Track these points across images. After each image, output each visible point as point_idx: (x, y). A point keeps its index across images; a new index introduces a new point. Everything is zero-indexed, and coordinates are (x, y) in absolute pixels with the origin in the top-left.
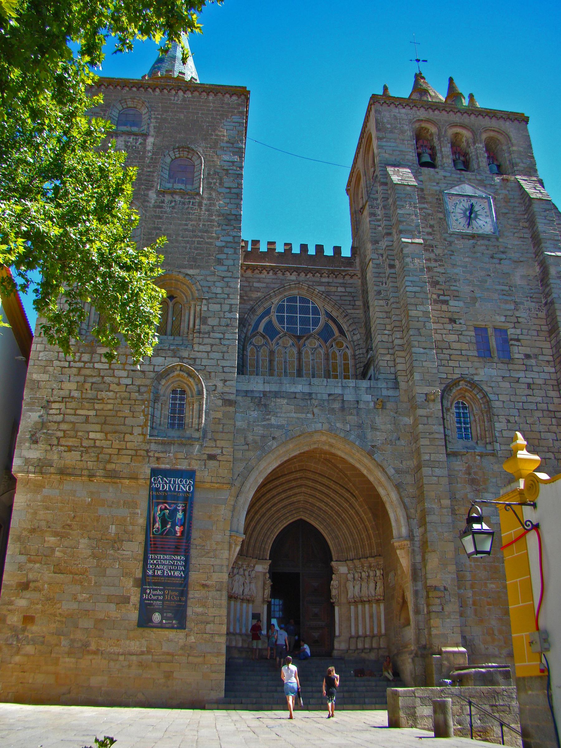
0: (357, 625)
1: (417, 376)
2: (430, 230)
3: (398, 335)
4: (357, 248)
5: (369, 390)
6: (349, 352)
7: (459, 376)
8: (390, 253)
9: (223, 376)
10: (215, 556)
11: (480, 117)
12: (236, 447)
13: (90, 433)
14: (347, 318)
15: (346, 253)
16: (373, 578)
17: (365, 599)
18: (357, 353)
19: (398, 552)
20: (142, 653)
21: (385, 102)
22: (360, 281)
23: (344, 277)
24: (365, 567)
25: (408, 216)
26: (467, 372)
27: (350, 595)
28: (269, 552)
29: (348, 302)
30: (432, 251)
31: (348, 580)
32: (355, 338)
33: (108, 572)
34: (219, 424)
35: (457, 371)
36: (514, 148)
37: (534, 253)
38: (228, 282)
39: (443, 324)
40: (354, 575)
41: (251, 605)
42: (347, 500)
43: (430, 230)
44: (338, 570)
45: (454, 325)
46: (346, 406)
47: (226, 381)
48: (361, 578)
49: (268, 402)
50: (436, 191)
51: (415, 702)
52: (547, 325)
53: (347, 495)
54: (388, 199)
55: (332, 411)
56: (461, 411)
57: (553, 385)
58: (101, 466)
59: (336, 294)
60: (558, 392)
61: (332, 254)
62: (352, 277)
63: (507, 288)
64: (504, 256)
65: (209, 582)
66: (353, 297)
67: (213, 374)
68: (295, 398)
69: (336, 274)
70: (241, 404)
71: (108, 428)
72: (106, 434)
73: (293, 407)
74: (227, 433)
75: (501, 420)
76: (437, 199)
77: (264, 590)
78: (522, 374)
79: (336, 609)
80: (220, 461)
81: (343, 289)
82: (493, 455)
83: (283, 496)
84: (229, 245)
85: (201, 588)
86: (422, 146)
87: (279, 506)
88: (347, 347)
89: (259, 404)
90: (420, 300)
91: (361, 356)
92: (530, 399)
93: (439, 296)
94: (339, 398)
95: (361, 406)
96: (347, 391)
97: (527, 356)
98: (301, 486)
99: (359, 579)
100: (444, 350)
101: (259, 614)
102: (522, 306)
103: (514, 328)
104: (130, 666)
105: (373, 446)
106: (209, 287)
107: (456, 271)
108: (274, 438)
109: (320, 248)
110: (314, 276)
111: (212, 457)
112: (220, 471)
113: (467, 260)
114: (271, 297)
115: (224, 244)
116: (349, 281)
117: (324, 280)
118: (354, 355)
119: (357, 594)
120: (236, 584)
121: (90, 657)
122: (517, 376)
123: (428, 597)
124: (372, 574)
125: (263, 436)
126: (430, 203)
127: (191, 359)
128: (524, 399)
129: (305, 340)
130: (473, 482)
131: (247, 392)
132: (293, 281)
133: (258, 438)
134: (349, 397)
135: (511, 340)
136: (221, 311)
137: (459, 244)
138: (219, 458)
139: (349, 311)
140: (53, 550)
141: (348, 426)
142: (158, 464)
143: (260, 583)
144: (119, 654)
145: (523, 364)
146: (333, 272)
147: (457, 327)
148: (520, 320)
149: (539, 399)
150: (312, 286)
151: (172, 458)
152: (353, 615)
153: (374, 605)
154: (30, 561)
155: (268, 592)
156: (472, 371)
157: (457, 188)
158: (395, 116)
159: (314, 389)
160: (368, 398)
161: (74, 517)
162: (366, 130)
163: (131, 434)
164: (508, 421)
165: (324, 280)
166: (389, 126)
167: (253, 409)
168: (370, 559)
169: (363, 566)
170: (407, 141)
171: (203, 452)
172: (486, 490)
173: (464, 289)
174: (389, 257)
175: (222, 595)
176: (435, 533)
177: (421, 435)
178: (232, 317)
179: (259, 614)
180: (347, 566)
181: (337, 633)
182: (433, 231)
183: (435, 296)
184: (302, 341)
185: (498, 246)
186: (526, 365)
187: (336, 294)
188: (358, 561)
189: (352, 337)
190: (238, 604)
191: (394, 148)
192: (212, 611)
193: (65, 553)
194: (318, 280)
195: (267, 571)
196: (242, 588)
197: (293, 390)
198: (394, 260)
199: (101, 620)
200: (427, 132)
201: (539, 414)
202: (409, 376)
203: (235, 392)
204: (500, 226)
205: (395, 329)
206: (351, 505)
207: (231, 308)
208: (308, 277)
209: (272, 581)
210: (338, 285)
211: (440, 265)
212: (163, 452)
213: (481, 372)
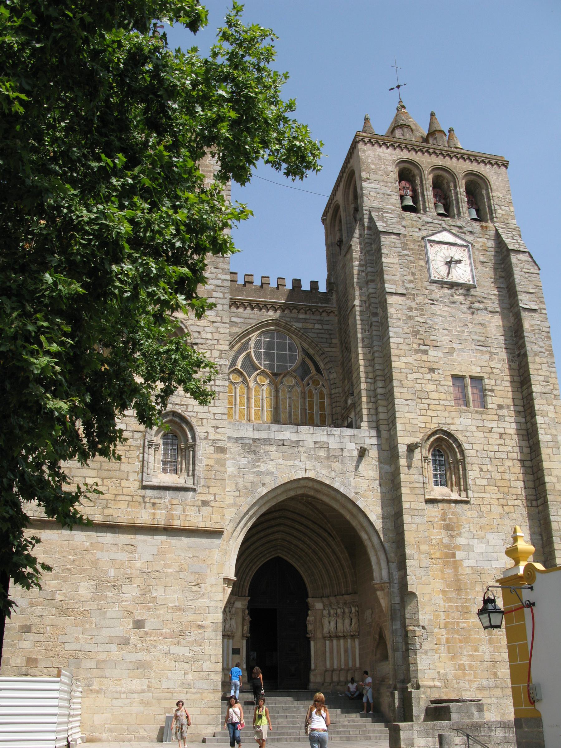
0: (332, 659)
1: (399, 427)
2: (412, 278)
3: (380, 384)
4: (334, 283)
5: (352, 438)
6: (325, 391)
7: (437, 425)
8: (373, 300)
9: (214, 423)
10: (210, 598)
11: (461, 160)
13: (87, 479)
14: (324, 356)
15: (323, 288)
17: (340, 635)
18: (333, 391)
19: (379, 593)
20: (143, 691)
21: (370, 140)
22: (336, 318)
23: (321, 314)
25: (392, 266)
26: (444, 422)
27: (326, 630)
29: (324, 340)
30: (414, 299)
31: (323, 616)
32: (332, 376)
33: (109, 614)
35: (435, 420)
36: (494, 194)
37: (510, 304)
38: (217, 328)
39: (422, 373)
41: (231, 641)
42: (324, 539)
43: (412, 278)
44: (314, 606)
45: (433, 375)
46: (331, 455)
47: (218, 428)
49: (258, 449)
50: (418, 237)
51: (413, 735)
52: (520, 376)
53: (325, 535)
54: (372, 244)
55: (318, 458)
56: (437, 458)
57: (523, 435)
58: (99, 510)
59: (313, 331)
60: (527, 442)
61: (309, 289)
62: (328, 314)
63: (483, 339)
64: (481, 306)
65: (204, 624)
66: (330, 334)
67: (204, 421)
68: (283, 445)
69: (313, 310)
70: (232, 451)
71: (104, 474)
72: (103, 479)
73: (281, 454)
75: (474, 468)
76: (419, 246)
77: (243, 625)
78: (494, 424)
79: (312, 643)
80: (213, 507)
81: (320, 327)
82: (467, 502)
83: (262, 534)
84: (219, 289)
85: (197, 629)
86: (404, 188)
87: (258, 544)
88: (323, 386)
89: (249, 451)
90: (403, 351)
91: (337, 395)
92: (502, 448)
93: (420, 345)
94: (325, 446)
95: (346, 453)
96: (332, 439)
97: (500, 407)
98: (279, 525)
100: (423, 400)
101: (239, 649)
102: (496, 357)
103: (489, 378)
104: (131, 703)
105: (356, 493)
106: (199, 332)
107: (436, 320)
108: (264, 485)
109: (297, 283)
110: (291, 312)
111: (205, 503)
112: (213, 516)
113: (446, 309)
114: (249, 334)
115: (212, 287)
116: (327, 318)
117: (302, 316)
118: (331, 394)
121: (94, 695)
122: (490, 426)
124: (347, 610)
125: (253, 483)
126: (412, 249)
127: (182, 405)
128: (496, 448)
129: (283, 377)
130: (448, 527)
131: (237, 439)
132: (270, 316)
133: (248, 485)
134: (334, 444)
135: (486, 390)
136: (211, 357)
137: (439, 293)
138: (212, 504)
139: (326, 349)
140: (54, 594)
141: (333, 474)
142: (154, 509)
143: (240, 620)
144: (121, 693)
145: (496, 414)
146: (310, 308)
147: (435, 376)
148: (494, 370)
149: (510, 449)
150: (290, 322)
151: (168, 503)
152: (328, 649)
153: (349, 640)
154: (31, 604)
155: (247, 628)
156: (449, 421)
157: (438, 235)
158: (379, 156)
159: (301, 437)
160: (352, 446)
161: (74, 561)
162: (349, 166)
163: (127, 480)
164: (481, 470)
165: (302, 316)
166: (373, 167)
167: (243, 456)
168: (346, 597)
169: (338, 603)
170: (392, 183)
171: (196, 498)
172: (459, 535)
173: (443, 339)
174: (373, 305)
175: (217, 635)
176: (414, 577)
177: (403, 484)
178: (222, 363)
179: (239, 649)
180: (323, 602)
181: (313, 667)
182: (415, 279)
183: (415, 346)
184: (279, 379)
185: (475, 296)
186: (499, 416)
187: (313, 331)
188: (334, 598)
189: (328, 376)
191: (379, 191)
192: (208, 651)
193: (66, 597)
194: (295, 316)
197: (281, 436)
198: (376, 308)
199: (104, 661)
200: (410, 173)
201: (509, 463)
202: (391, 425)
203: (226, 439)
204: (478, 275)
205: (378, 378)
206: (328, 544)
207: (221, 354)
208: (286, 312)
209: (251, 617)
210: (315, 321)
211: (420, 314)
212: (159, 498)
213: (457, 421)
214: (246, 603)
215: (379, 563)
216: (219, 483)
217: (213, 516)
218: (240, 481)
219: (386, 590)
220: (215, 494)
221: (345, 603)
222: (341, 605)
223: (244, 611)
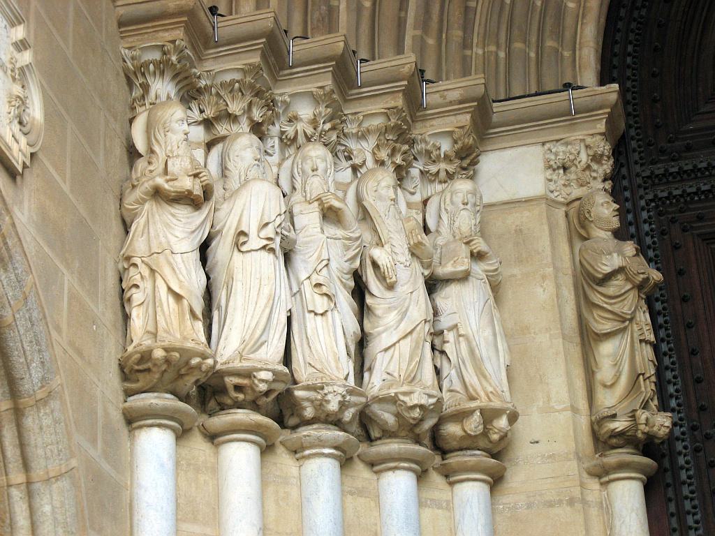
77: (588, 339)
223: (579, 226)
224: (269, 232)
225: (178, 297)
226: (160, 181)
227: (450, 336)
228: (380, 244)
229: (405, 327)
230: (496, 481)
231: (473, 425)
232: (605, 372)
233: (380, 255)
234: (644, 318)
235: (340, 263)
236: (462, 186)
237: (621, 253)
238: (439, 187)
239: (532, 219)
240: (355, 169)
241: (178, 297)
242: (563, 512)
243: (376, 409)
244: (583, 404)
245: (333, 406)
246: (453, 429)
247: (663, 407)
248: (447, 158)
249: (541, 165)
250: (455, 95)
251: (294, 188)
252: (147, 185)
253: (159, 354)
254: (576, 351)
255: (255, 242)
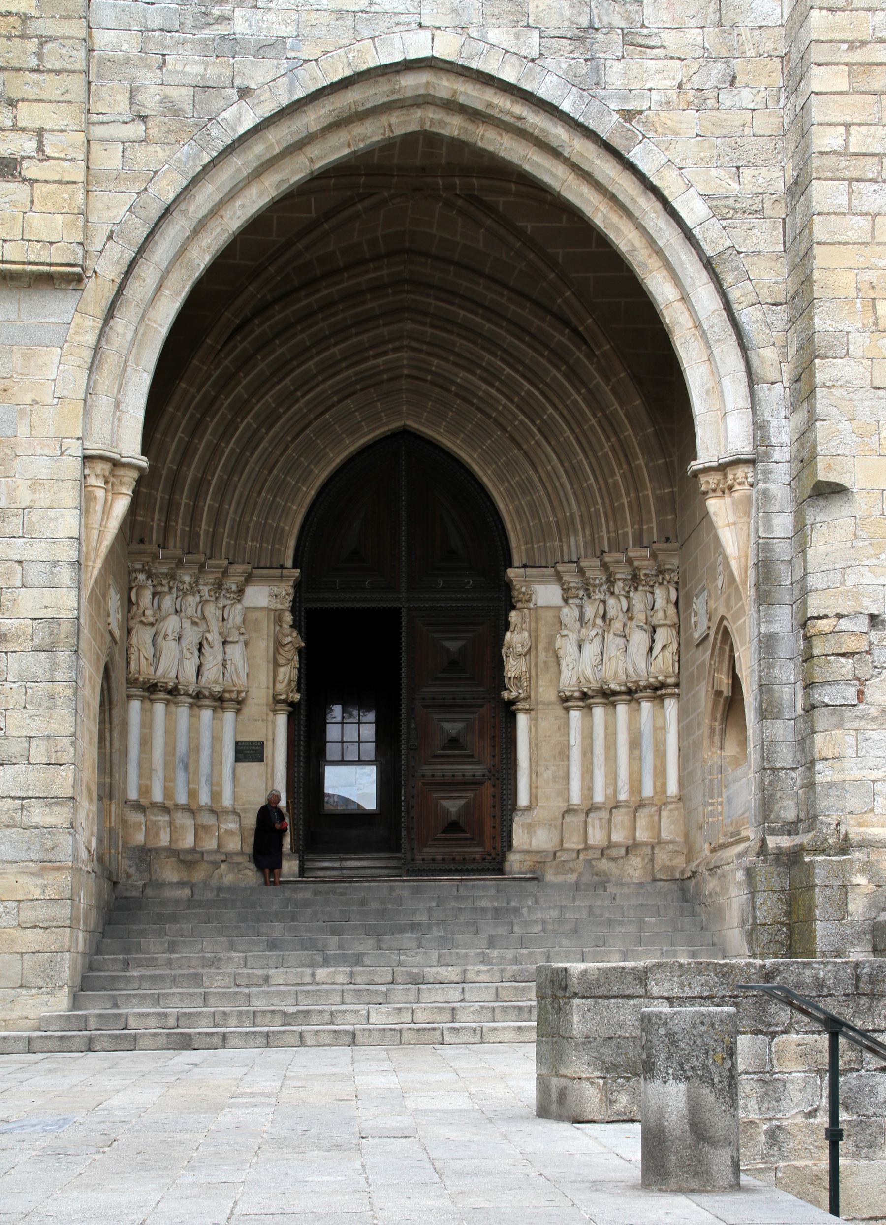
12: (99, 131)
16: (642, 617)
24: (620, 584)
28: (292, 543)
34: (23, 37)
40: (581, 607)
41: (229, 717)
48: (604, 617)
74: (58, 72)
77: (276, 665)
80: (32, 182)
99: (599, 622)
108: (244, 93)
112: (35, 219)
119: (589, 672)
120: (169, 648)
123: (808, 657)
133: (182, 95)
138: (30, 169)
143: (263, 646)
155: (288, 672)
169: (611, 581)
190: (183, 712)
195: (287, 605)
196: (195, 661)
214: (286, 589)
215: (717, 390)
216: (52, 86)
217: (35, 219)
218: (149, 78)
219: (741, 491)
220: (40, 132)
221: (635, 580)
222: (619, 587)
223: (279, 620)
224: (175, 634)
225: (147, 659)
226: (143, 619)
227: (229, 662)
228: (209, 631)
229: (215, 662)
230: (238, 711)
231: (234, 696)
232: (280, 677)
233: (208, 635)
234: (297, 658)
235: (196, 641)
236: (239, 606)
237: (291, 635)
238: (230, 602)
239: (261, 616)
240: (201, 597)
241: (147, 659)
242: (259, 724)
243: (203, 690)
244: (271, 686)
245: (190, 692)
246: (227, 695)
247: (298, 691)
248: (234, 593)
249: (268, 594)
250: (241, 570)
251: (181, 610)
252: (139, 620)
253: (141, 679)
254: (271, 666)
255: (170, 637)
